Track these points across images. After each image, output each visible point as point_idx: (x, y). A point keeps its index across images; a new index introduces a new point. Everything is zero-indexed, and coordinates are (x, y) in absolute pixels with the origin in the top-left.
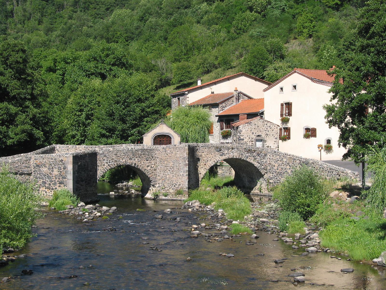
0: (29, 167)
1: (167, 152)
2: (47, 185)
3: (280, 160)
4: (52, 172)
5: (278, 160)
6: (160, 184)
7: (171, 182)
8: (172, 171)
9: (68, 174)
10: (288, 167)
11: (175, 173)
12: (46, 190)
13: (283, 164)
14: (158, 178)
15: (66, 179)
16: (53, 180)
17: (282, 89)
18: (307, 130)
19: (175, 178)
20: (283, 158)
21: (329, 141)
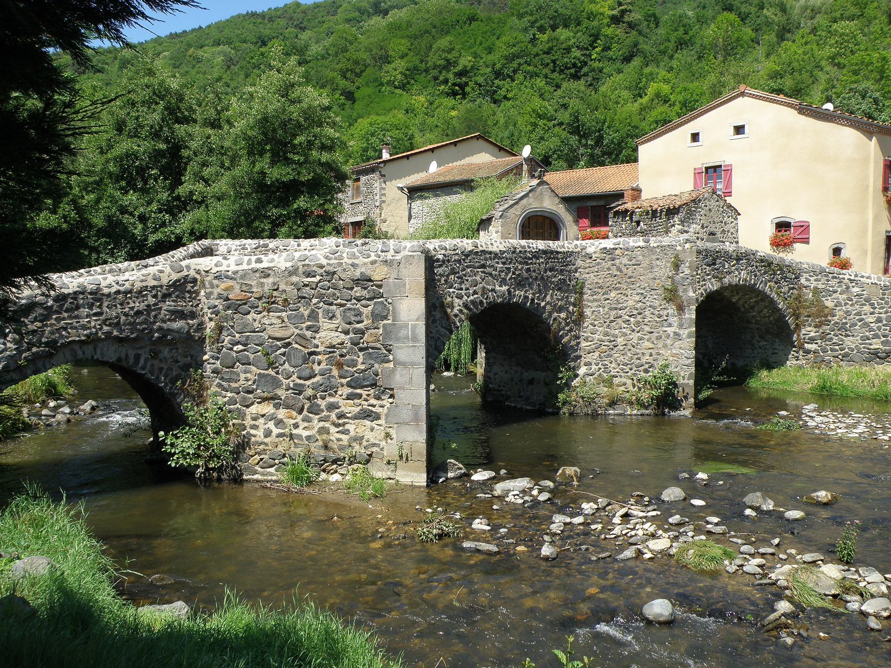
0: (193, 315)
1: (617, 262)
2: (281, 392)
3: (839, 289)
4: (309, 334)
5: (835, 292)
6: (594, 367)
7: (632, 358)
8: (638, 323)
9: (398, 340)
10: (867, 308)
11: (647, 329)
12: (282, 413)
13: (851, 300)
14: (584, 344)
15: (391, 365)
16: (317, 368)
17: (695, 137)
18: (783, 226)
20: (851, 285)
21: (837, 251)
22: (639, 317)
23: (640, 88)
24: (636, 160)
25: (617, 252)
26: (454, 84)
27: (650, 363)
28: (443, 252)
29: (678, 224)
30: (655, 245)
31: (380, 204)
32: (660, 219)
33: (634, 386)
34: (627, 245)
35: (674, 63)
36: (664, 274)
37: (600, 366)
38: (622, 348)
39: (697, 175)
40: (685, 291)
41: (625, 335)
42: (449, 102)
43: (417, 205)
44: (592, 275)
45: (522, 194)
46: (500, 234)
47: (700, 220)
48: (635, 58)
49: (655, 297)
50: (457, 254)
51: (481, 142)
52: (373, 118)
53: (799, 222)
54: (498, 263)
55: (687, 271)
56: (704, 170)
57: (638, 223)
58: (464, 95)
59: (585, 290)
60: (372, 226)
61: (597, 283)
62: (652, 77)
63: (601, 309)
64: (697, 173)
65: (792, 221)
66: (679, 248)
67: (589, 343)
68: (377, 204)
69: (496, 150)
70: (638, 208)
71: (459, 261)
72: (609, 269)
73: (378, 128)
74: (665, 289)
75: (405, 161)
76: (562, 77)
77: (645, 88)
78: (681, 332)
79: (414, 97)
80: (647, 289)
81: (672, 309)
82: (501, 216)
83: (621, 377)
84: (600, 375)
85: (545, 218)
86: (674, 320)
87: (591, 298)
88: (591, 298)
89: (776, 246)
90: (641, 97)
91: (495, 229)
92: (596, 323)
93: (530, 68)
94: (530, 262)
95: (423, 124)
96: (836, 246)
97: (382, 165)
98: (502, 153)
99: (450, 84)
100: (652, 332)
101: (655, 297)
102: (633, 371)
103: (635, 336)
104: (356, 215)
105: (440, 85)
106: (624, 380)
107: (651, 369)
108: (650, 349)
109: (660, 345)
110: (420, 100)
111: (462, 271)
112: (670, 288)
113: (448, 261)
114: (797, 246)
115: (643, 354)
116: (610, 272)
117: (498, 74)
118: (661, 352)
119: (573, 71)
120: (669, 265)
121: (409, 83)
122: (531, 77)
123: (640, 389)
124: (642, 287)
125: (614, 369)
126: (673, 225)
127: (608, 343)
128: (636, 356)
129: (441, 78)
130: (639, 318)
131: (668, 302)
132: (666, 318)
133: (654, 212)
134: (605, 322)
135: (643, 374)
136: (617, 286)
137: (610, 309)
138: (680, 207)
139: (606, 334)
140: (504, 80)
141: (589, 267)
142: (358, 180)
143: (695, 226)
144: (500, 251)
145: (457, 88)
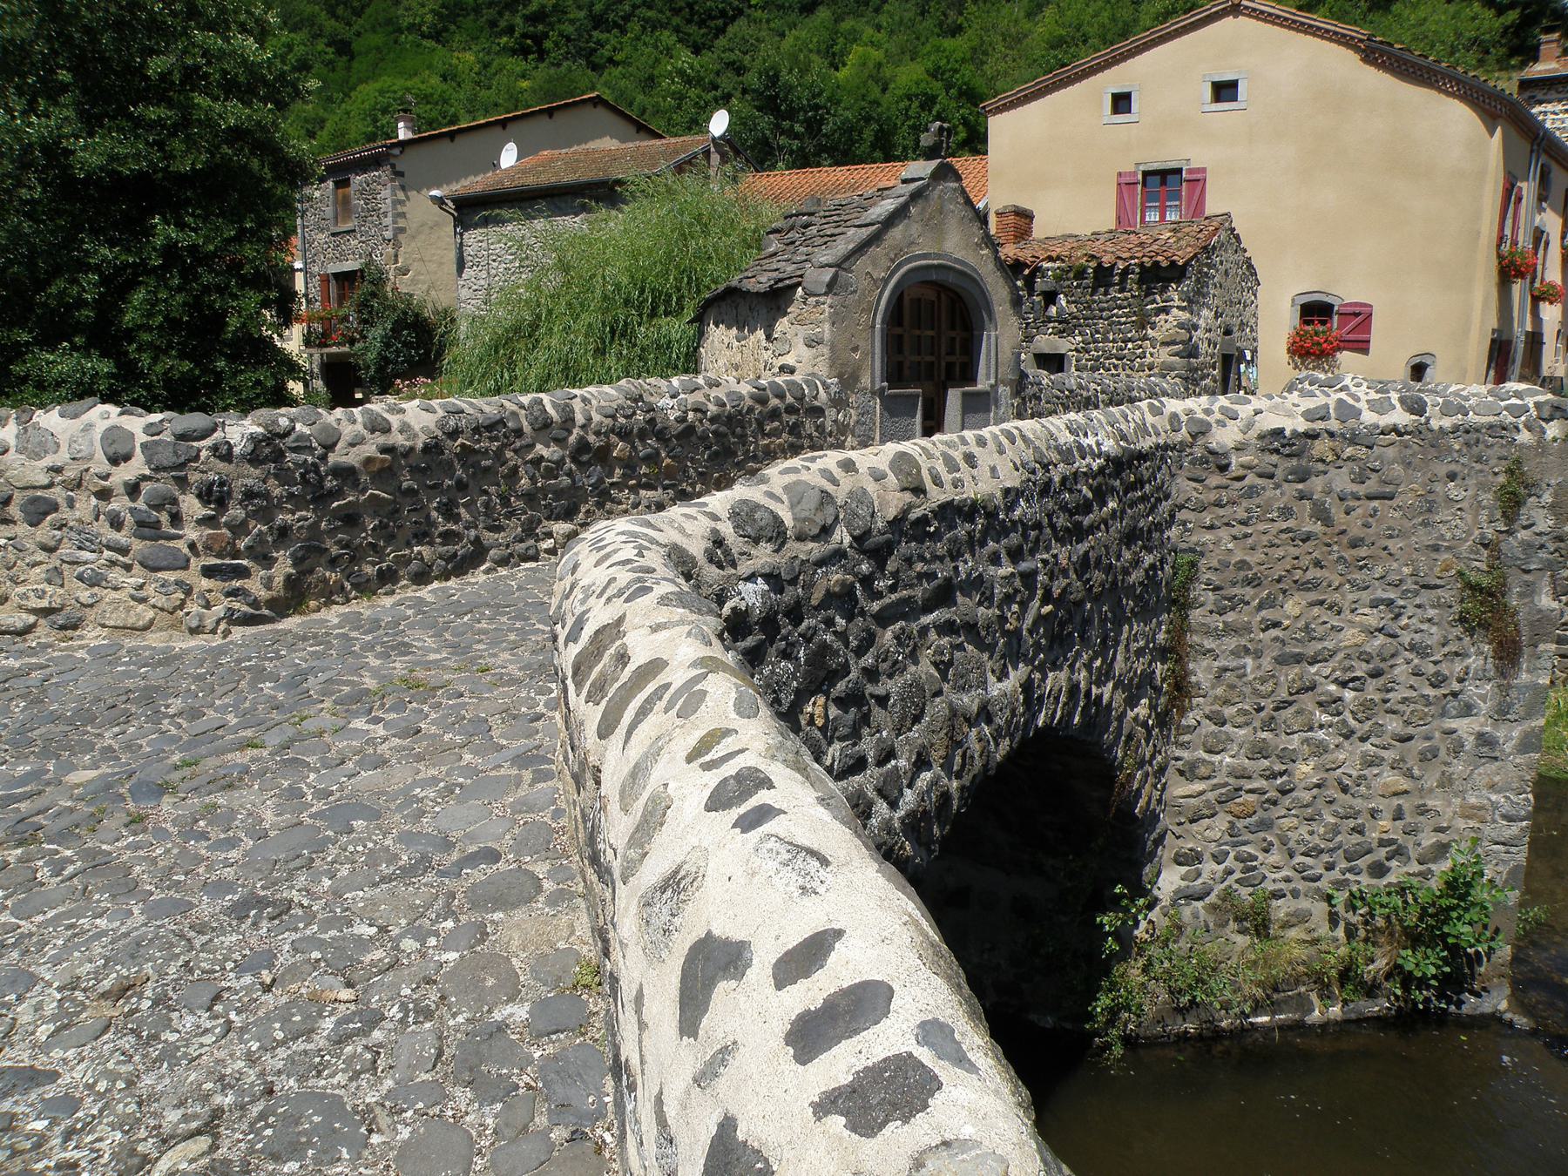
1: (1316, 484)
6: (1209, 867)
7: (1335, 831)
11: (1393, 725)
14: (1179, 789)
17: (1121, 102)
19: (1391, 779)
22: (1372, 684)
23: (834, 54)
24: (986, 153)
25: (1321, 447)
26: (525, 36)
27: (1391, 842)
28: (764, 556)
29: (1178, 307)
30: (1447, 423)
31: (395, 236)
32: (1122, 290)
33: (1333, 920)
34: (1351, 423)
35: (883, 19)
36: (1469, 533)
37: (1230, 862)
38: (1306, 797)
39: (1124, 188)
40: (1530, 591)
41: (1320, 749)
42: (515, 64)
43: (473, 237)
44: (1224, 533)
45: (888, 205)
46: (825, 350)
47: (1214, 296)
48: (821, 8)
49: (1431, 613)
50: (839, 555)
51: (601, 113)
52: (385, 81)
53: (1351, 305)
54: (995, 560)
55: (1544, 523)
56: (1140, 177)
57: (1050, 297)
58: (542, 55)
59: (1199, 591)
60: (379, 281)
61: (1243, 565)
62: (853, 37)
63: (1249, 661)
64: (1125, 185)
65: (1336, 303)
66: (1524, 437)
67: (1198, 786)
68: (388, 234)
69: (632, 130)
70: (1050, 259)
71: (843, 600)
72: (1286, 512)
73: (395, 100)
74: (1470, 586)
75: (445, 145)
76: (703, 31)
77: (844, 52)
78: (1500, 734)
79: (456, 54)
80: (1409, 585)
81: (1480, 655)
82: (831, 286)
83: (1295, 894)
84: (1227, 895)
85: (940, 287)
86: (1481, 693)
87: (1218, 622)
88: (1218, 622)
89: (1300, 356)
90: (837, 69)
91: (804, 331)
92: (1229, 711)
93: (650, 14)
94: (1087, 521)
95: (472, 100)
96: (1418, 360)
97: (396, 151)
98: (642, 134)
99: (517, 34)
100: (1410, 738)
101: (1431, 613)
102: (1336, 874)
103: (1349, 757)
104: (342, 257)
105: (500, 35)
106: (1304, 904)
107: (1394, 863)
108: (1396, 794)
109: (1431, 781)
110: (468, 59)
111: (860, 652)
112: (1485, 581)
113: (795, 613)
114: (1345, 357)
115: (1374, 813)
116: (1291, 523)
117: (599, 22)
118: (1430, 803)
119: (720, 22)
120: (1487, 498)
121: (446, 29)
122: (654, 28)
123: (1351, 933)
124: (1394, 577)
125: (1274, 869)
126: (1166, 310)
127: (1260, 783)
128: (1351, 823)
129: (503, 24)
130: (1372, 691)
131: (1471, 631)
132: (1456, 686)
133: (1103, 276)
134: (1260, 709)
135: (1365, 879)
136: (1310, 575)
137: (1282, 661)
138: (1187, 263)
139: (1260, 751)
140: (609, 32)
141: (1218, 504)
142: (342, 184)
143: (1205, 312)
144: (1007, 491)
145: (529, 42)
